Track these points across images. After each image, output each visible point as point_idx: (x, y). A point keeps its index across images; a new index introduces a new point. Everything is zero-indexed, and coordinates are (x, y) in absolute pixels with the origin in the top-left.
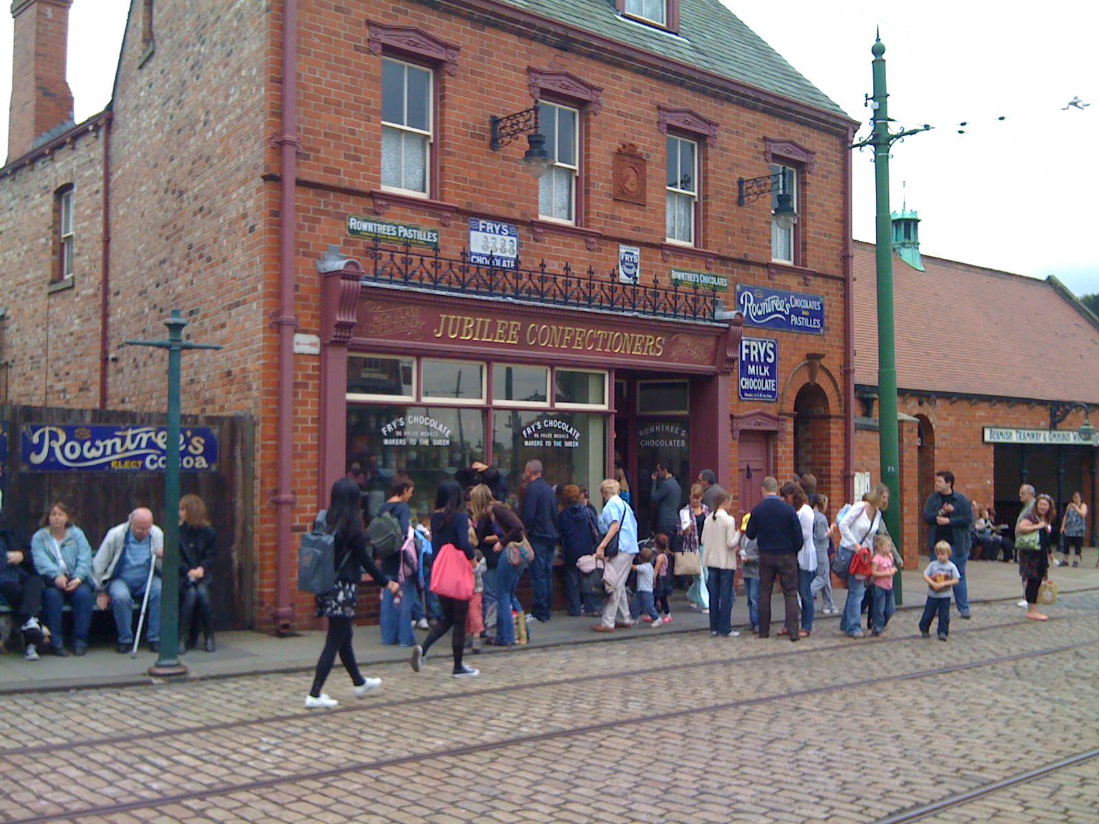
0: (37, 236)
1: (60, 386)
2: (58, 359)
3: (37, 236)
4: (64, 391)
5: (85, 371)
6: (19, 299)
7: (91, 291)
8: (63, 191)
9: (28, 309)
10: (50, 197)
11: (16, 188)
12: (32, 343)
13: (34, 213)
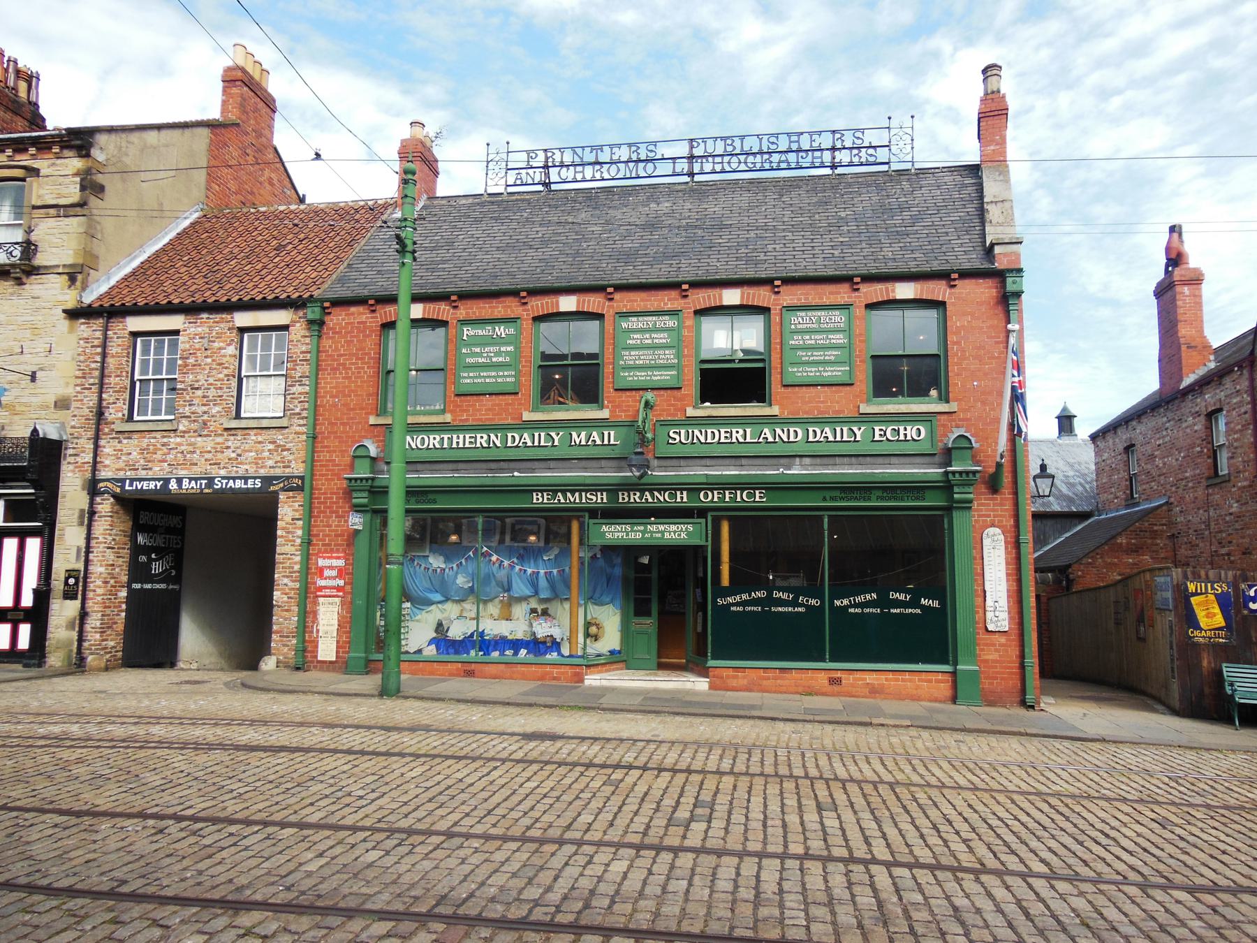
0: (1193, 446)
1: (1224, 551)
2: (1221, 532)
3: (1193, 446)
4: (1228, 554)
5: (1247, 540)
6: (1180, 491)
7: (1245, 483)
8: (1212, 415)
9: (1189, 497)
10: (1202, 418)
11: (1170, 415)
12: (1196, 520)
13: (1188, 430)
